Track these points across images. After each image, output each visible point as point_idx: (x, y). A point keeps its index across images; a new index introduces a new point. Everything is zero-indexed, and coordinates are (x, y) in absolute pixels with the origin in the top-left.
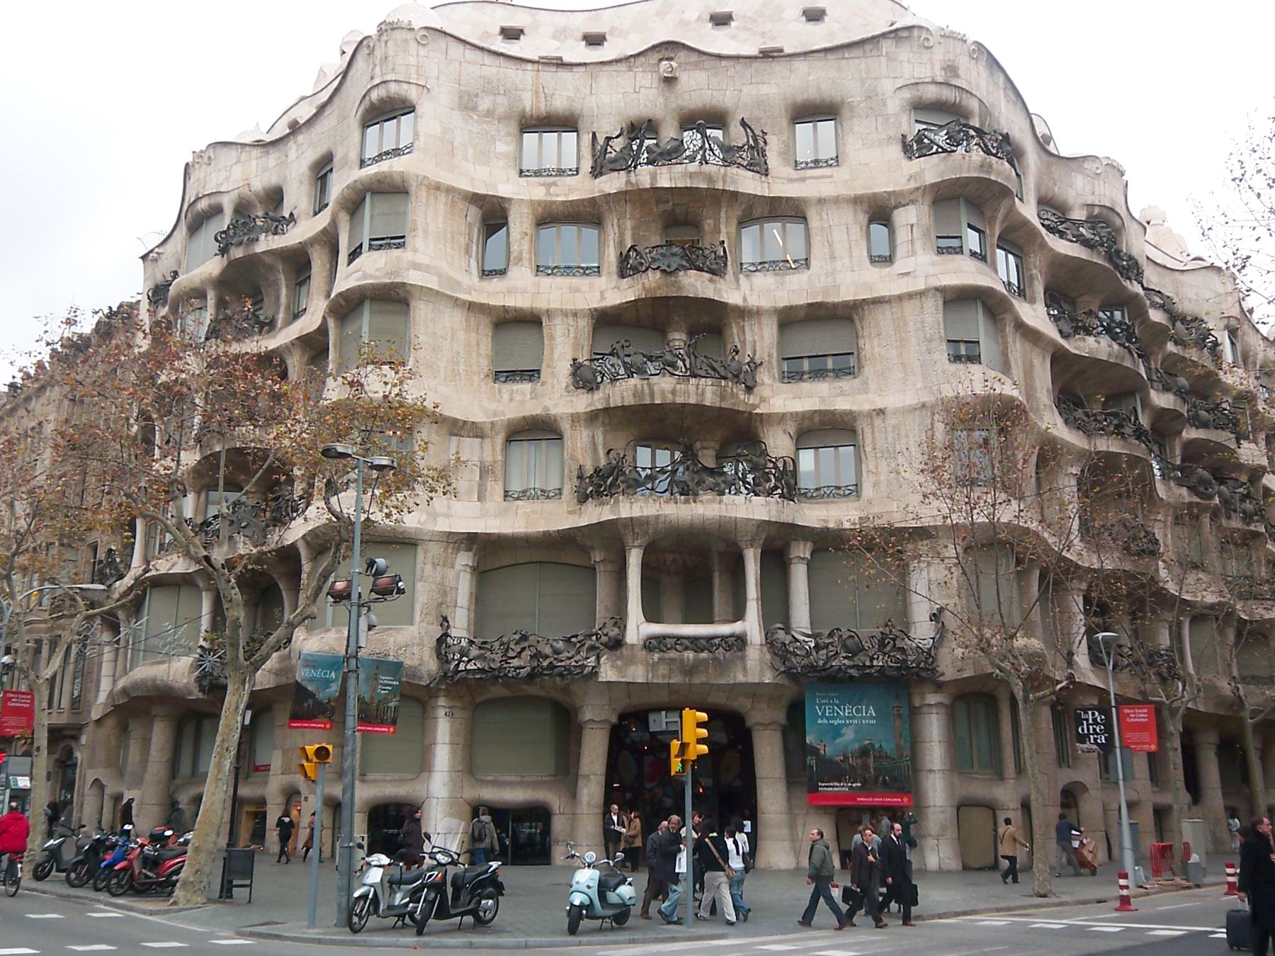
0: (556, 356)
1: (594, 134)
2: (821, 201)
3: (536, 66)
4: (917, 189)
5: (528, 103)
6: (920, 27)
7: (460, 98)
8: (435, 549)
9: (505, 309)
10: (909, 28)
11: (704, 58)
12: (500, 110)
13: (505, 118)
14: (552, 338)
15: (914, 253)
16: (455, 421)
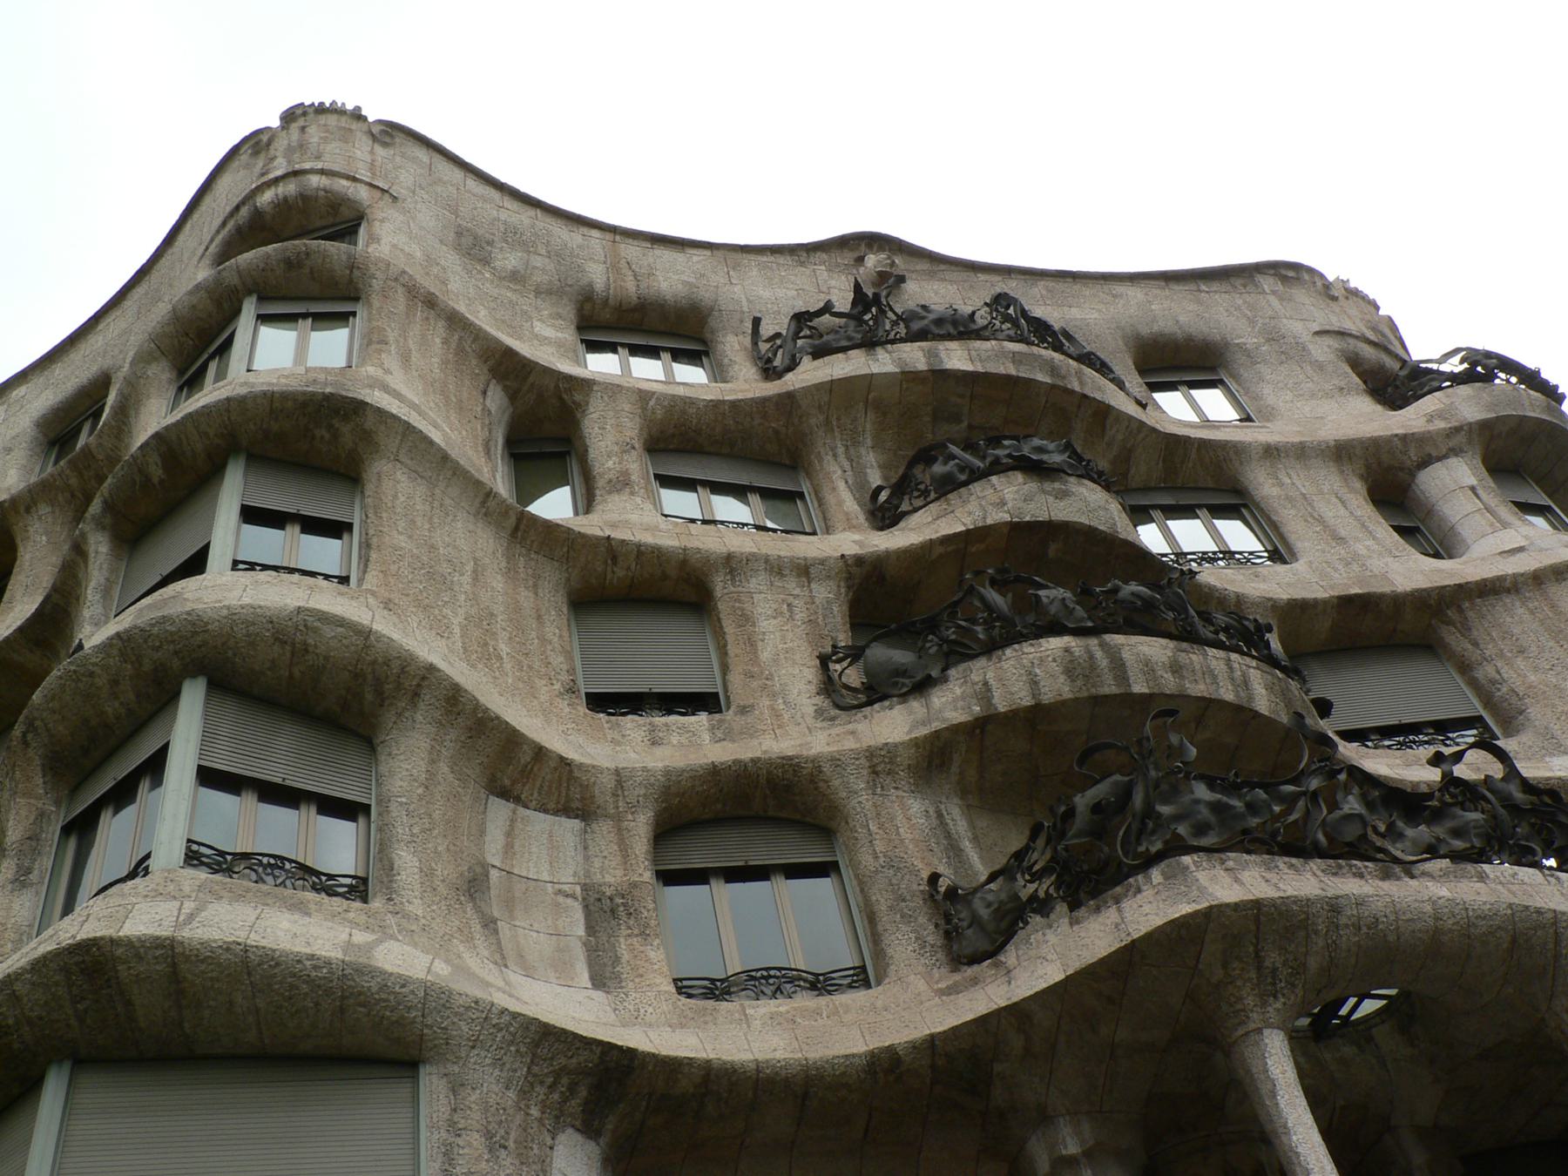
0: (765, 655)
1: (757, 322)
2: (1272, 453)
3: (609, 236)
4: (1458, 429)
5: (597, 275)
6: (1311, 271)
7: (459, 234)
8: (490, 1085)
9: (610, 549)
10: (1296, 267)
11: (942, 267)
12: (538, 278)
13: (549, 292)
14: (746, 619)
15: (1505, 525)
16: (512, 739)
